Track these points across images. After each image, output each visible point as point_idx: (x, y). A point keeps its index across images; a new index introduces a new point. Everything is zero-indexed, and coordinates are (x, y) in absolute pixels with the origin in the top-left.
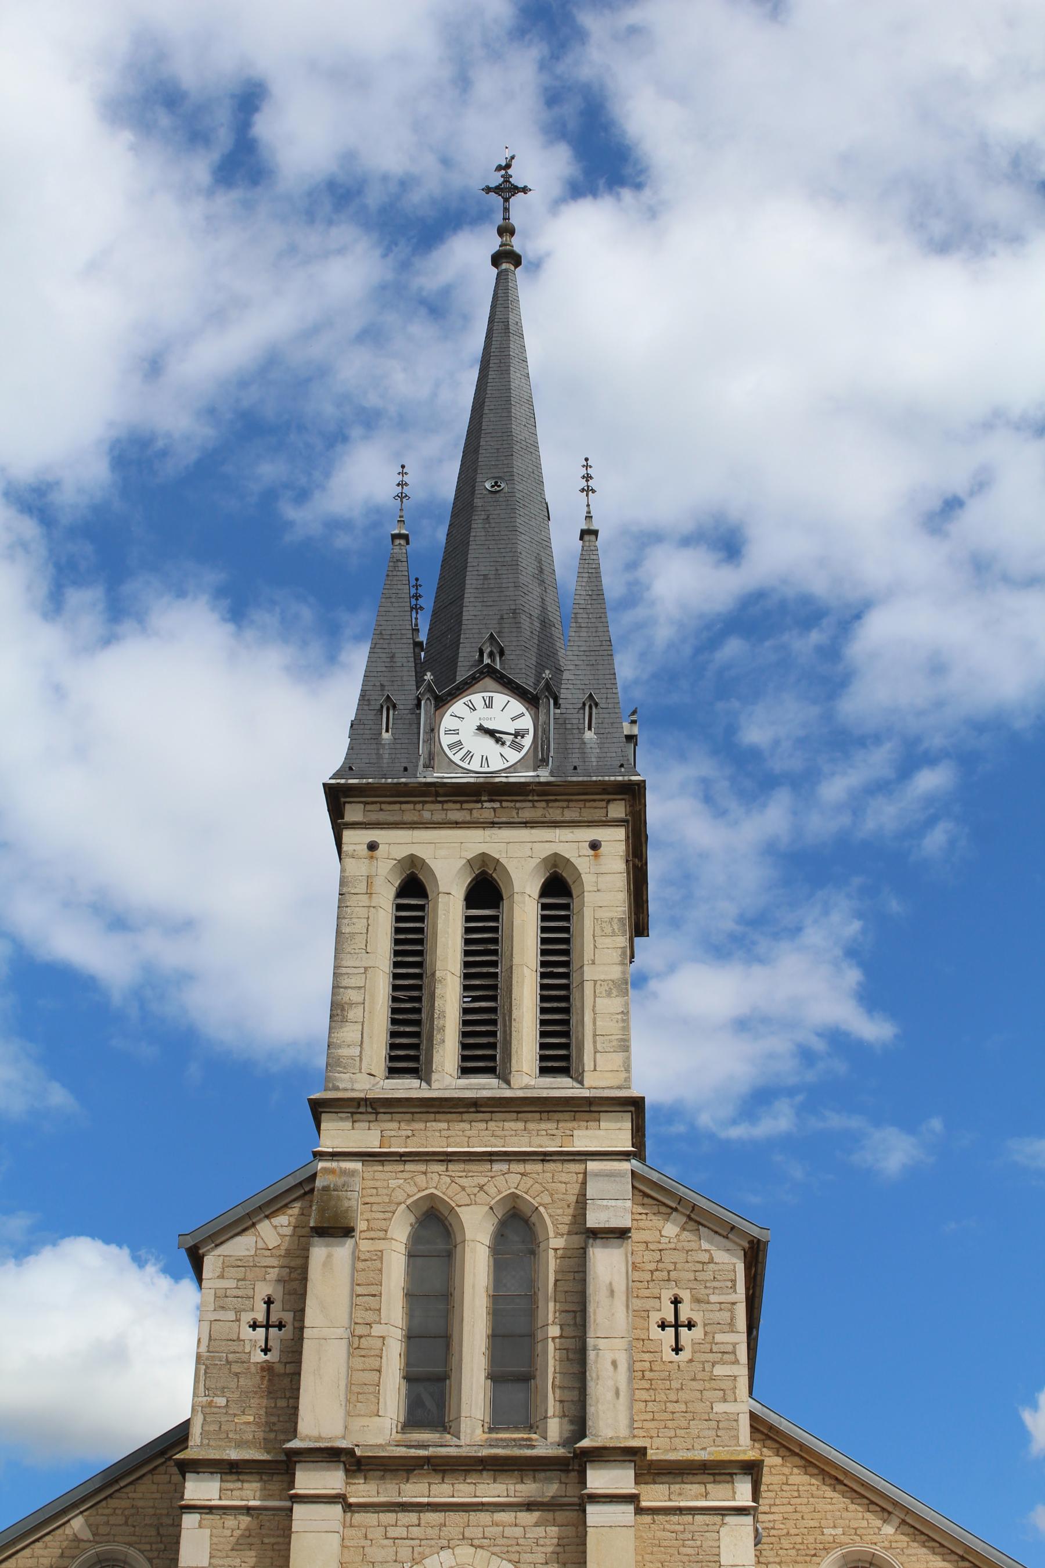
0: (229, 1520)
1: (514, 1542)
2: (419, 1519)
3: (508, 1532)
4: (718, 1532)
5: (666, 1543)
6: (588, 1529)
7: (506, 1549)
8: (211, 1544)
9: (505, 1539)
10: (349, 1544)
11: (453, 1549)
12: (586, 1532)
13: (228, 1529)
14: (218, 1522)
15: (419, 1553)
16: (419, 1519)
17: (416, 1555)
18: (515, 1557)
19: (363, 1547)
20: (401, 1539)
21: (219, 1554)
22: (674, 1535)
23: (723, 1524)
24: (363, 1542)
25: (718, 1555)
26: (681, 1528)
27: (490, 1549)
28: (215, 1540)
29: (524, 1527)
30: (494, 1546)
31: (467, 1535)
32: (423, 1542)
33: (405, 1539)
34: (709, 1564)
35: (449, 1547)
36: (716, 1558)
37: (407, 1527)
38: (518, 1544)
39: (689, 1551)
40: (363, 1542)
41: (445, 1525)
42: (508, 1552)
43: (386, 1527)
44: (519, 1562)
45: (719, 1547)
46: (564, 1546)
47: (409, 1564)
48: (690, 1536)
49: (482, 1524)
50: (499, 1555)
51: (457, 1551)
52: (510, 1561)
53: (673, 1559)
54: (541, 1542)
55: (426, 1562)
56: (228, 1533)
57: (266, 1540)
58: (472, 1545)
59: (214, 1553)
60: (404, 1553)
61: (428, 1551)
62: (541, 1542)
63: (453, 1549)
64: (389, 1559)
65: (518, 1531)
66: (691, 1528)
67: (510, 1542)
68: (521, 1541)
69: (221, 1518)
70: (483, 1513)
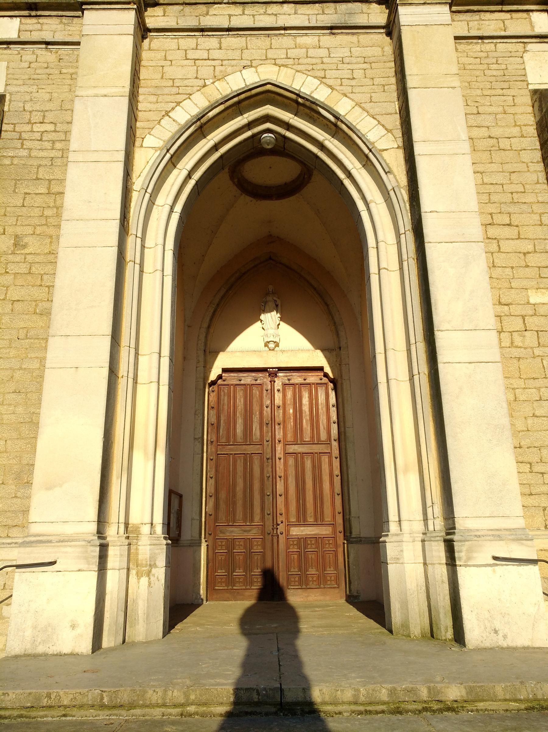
0: (27, 55)
1: (319, 61)
2: (220, 43)
3: (311, 52)
4: (522, 57)
5: (471, 67)
6: (402, 28)
7: (310, 68)
8: (7, 74)
9: (309, 59)
10: (146, 64)
11: (256, 67)
12: (400, 29)
13: (26, 62)
14: (16, 56)
15: (221, 72)
16: (220, 43)
17: (217, 73)
18: (322, 74)
19: (163, 67)
20: (202, 60)
21: (15, 82)
22: (478, 60)
23: (525, 51)
24: (163, 63)
25: (525, 75)
26: (484, 55)
27: (294, 67)
28: (11, 71)
29: (328, 49)
30: (299, 64)
31: (269, 56)
32: (225, 63)
33: (205, 60)
34: (517, 83)
35: (252, 66)
36: (523, 78)
37: (208, 50)
38: (322, 63)
39: (495, 73)
40: (163, 63)
41: (247, 48)
42: (313, 69)
43: (186, 50)
44: (325, 78)
45: (524, 69)
46: (371, 63)
47: (211, 81)
48: (494, 61)
49: (285, 46)
50: (305, 72)
51: (260, 69)
52: (315, 77)
53: (479, 79)
54: (346, 60)
55: (228, 78)
56: (26, 65)
57: (64, 71)
58: (275, 64)
59: (10, 82)
60: (206, 71)
61: (229, 69)
62: (346, 60)
63: (256, 67)
64: (189, 76)
65: (323, 52)
66: (495, 54)
67: (314, 61)
68: (325, 60)
69: (19, 53)
70: (285, 38)
